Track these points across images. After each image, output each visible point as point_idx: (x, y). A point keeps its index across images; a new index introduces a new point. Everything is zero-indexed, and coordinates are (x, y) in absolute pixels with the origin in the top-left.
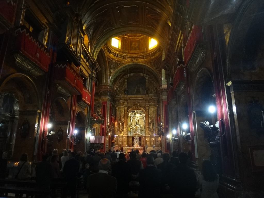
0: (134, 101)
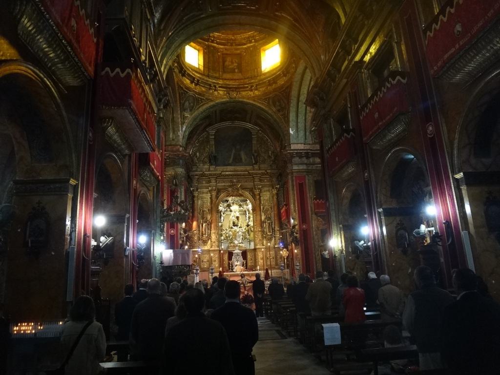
0: (230, 178)
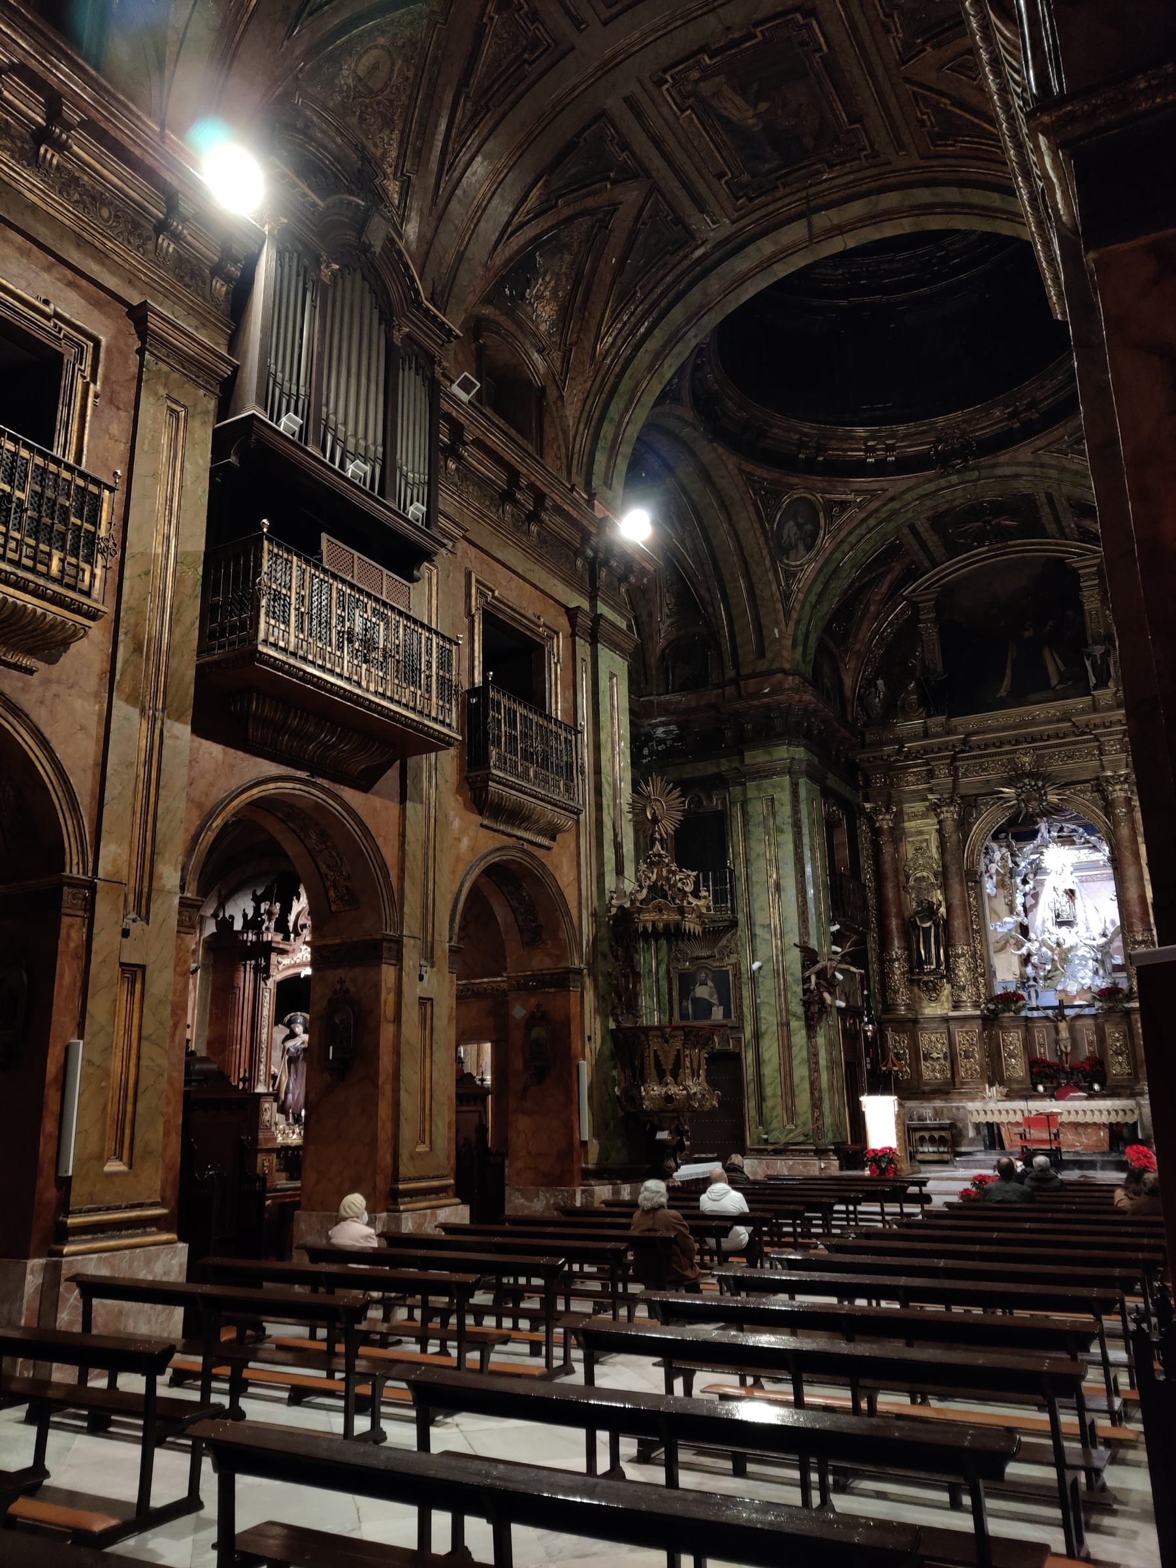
0: (1007, 753)
